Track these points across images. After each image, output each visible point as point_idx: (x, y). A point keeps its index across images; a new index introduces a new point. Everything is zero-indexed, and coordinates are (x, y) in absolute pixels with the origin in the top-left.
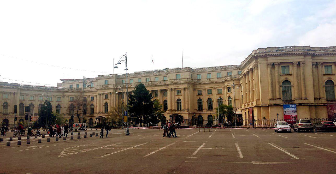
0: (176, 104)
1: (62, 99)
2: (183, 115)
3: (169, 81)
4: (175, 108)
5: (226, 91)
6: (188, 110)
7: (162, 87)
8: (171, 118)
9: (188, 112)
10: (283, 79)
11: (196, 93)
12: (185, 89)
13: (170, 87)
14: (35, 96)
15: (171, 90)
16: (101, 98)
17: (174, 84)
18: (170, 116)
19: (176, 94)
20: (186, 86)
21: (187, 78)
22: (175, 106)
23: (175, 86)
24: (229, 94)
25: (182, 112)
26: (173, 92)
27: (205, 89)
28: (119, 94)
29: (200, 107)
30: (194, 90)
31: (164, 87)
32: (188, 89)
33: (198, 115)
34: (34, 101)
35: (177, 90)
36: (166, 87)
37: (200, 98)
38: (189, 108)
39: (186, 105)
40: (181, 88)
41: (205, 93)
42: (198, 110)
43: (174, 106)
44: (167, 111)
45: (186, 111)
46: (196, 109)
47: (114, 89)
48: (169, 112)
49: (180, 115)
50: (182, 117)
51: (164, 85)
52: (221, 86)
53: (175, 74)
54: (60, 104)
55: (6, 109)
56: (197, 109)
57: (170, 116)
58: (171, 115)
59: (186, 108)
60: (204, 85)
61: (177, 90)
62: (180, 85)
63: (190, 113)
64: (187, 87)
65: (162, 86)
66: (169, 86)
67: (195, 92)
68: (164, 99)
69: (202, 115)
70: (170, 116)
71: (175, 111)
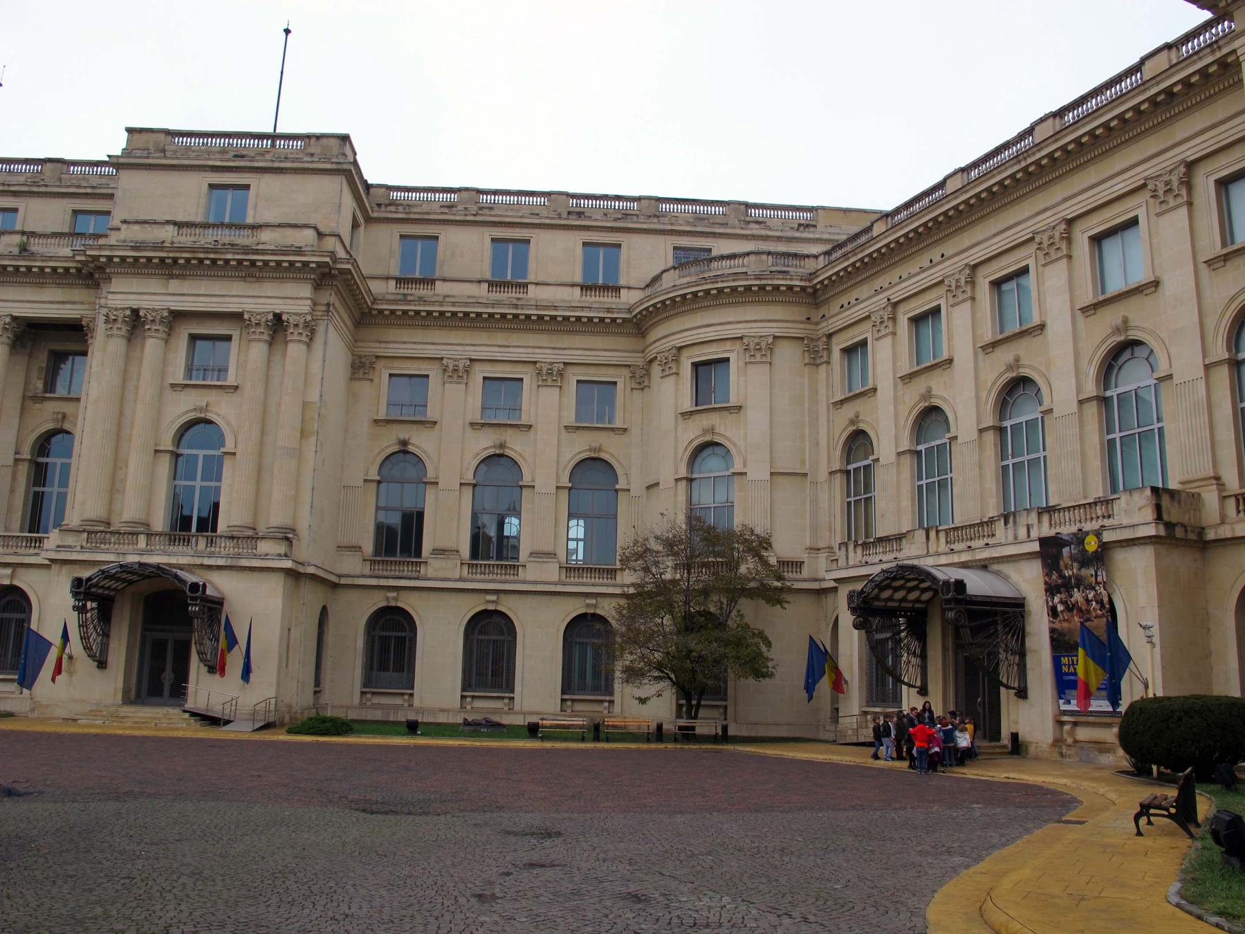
0: (164, 466)
2: (222, 584)
4: (149, 507)
5: (673, 392)
6: (287, 536)
8: (81, 610)
9: (288, 564)
11: (377, 395)
12: (278, 324)
13: (124, 293)
15: (136, 321)
17: (169, 266)
18: (78, 582)
19: (177, 374)
20: (293, 299)
21: (320, 235)
22: (151, 490)
23: (174, 285)
24: (705, 421)
25: (223, 553)
26: (152, 346)
27: (457, 373)
29: (401, 539)
30: (360, 367)
32: (311, 329)
33: (378, 601)
35: (194, 338)
36: (77, 294)
37: (404, 443)
38: (303, 525)
39: (277, 492)
40: (237, 317)
41: (455, 404)
42: (377, 552)
43: (146, 496)
44: (53, 538)
45: (264, 547)
46: (358, 548)
48: (70, 540)
49: (195, 587)
50: (215, 607)
52: (615, 358)
53: (196, 184)
56: (369, 547)
57: (81, 589)
58: (85, 574)
59: (276, 517)
60: (455, 336)
61: (194, 338)
62: (238, 287)
63: (311, 570)
64: (305, 306)
66: (117, 284)
67: (364, 388)
68: (43, 418)
69: (409, 603)
70: (78, 582)
71: (150, 535)
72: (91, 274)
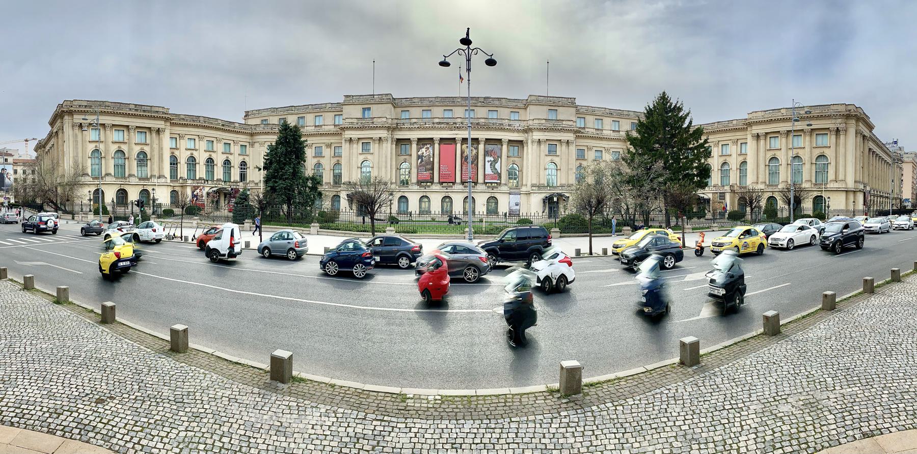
1: (249, 150)
3: (535, 121)
7: (512, 134)
10: (817, 152)
14: (197, 138)
16: (355, 151)
23: (546, 133)
28: (398, 140)
31: (516, 134)
34: (177, 149)
36: (521, 134)
47: (388, 128)
51: (518, 131)
54: (247, 160)
55: (143, 168)
65: (513, 131)
72: (527, 131)
